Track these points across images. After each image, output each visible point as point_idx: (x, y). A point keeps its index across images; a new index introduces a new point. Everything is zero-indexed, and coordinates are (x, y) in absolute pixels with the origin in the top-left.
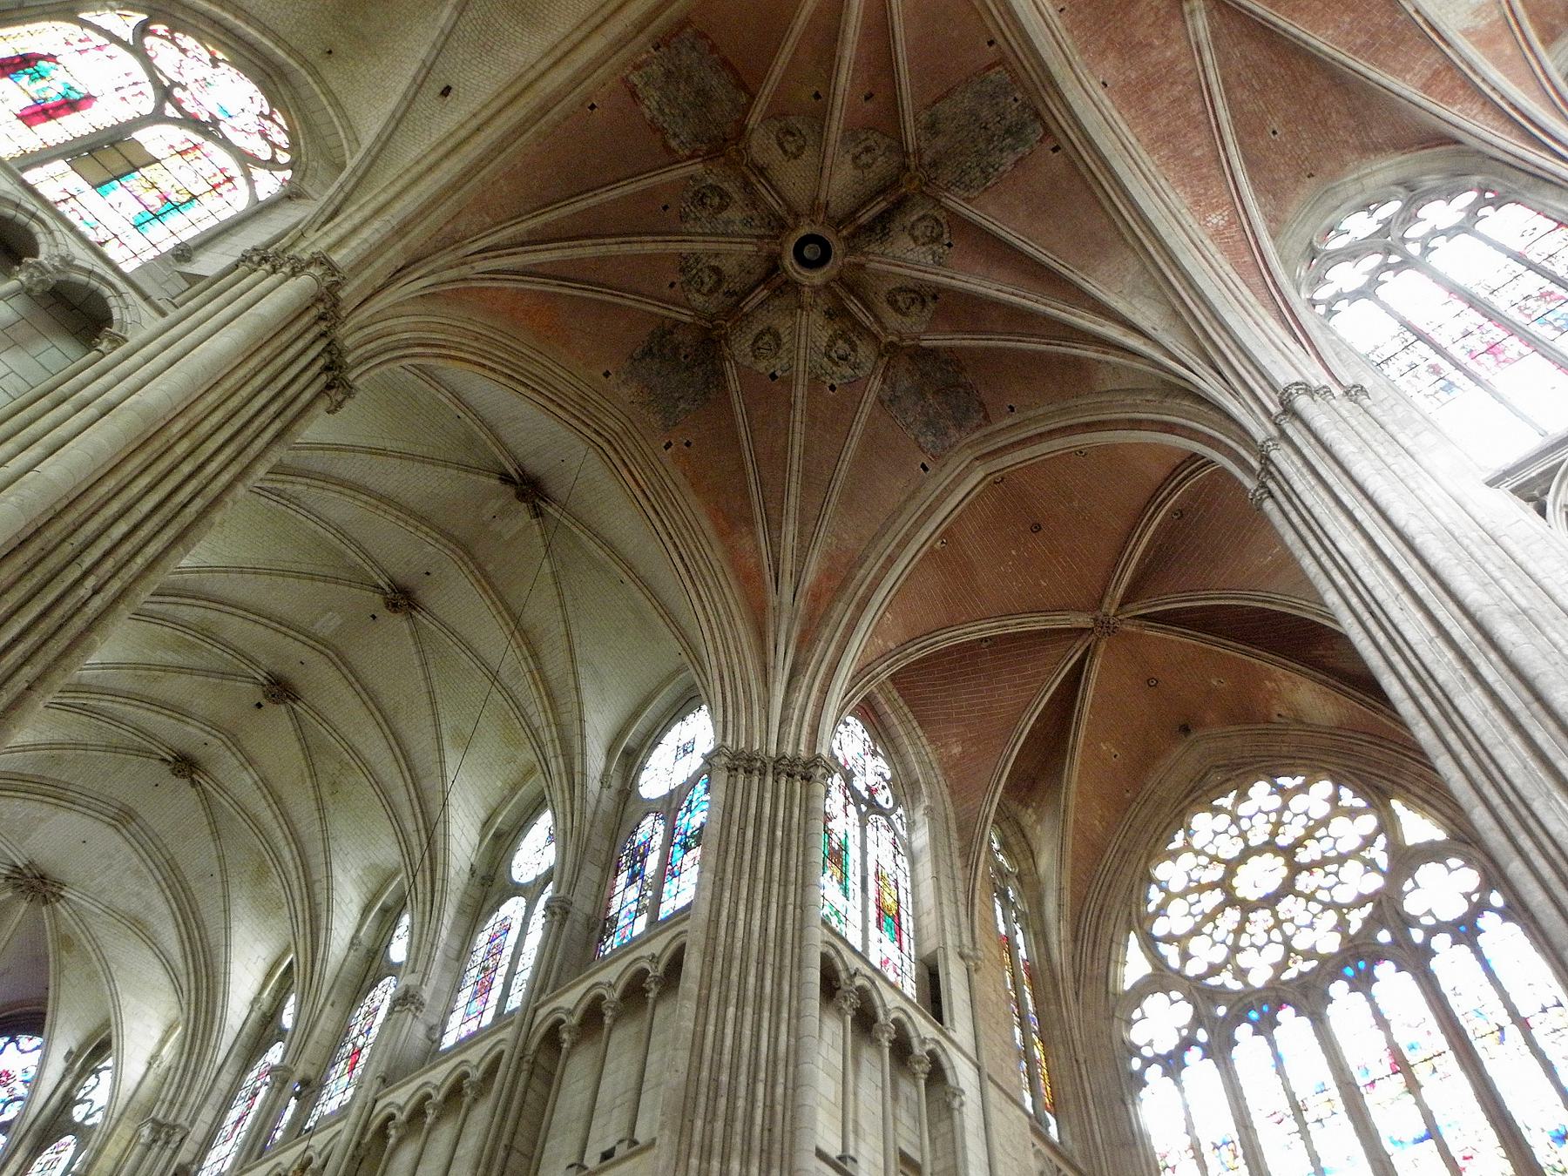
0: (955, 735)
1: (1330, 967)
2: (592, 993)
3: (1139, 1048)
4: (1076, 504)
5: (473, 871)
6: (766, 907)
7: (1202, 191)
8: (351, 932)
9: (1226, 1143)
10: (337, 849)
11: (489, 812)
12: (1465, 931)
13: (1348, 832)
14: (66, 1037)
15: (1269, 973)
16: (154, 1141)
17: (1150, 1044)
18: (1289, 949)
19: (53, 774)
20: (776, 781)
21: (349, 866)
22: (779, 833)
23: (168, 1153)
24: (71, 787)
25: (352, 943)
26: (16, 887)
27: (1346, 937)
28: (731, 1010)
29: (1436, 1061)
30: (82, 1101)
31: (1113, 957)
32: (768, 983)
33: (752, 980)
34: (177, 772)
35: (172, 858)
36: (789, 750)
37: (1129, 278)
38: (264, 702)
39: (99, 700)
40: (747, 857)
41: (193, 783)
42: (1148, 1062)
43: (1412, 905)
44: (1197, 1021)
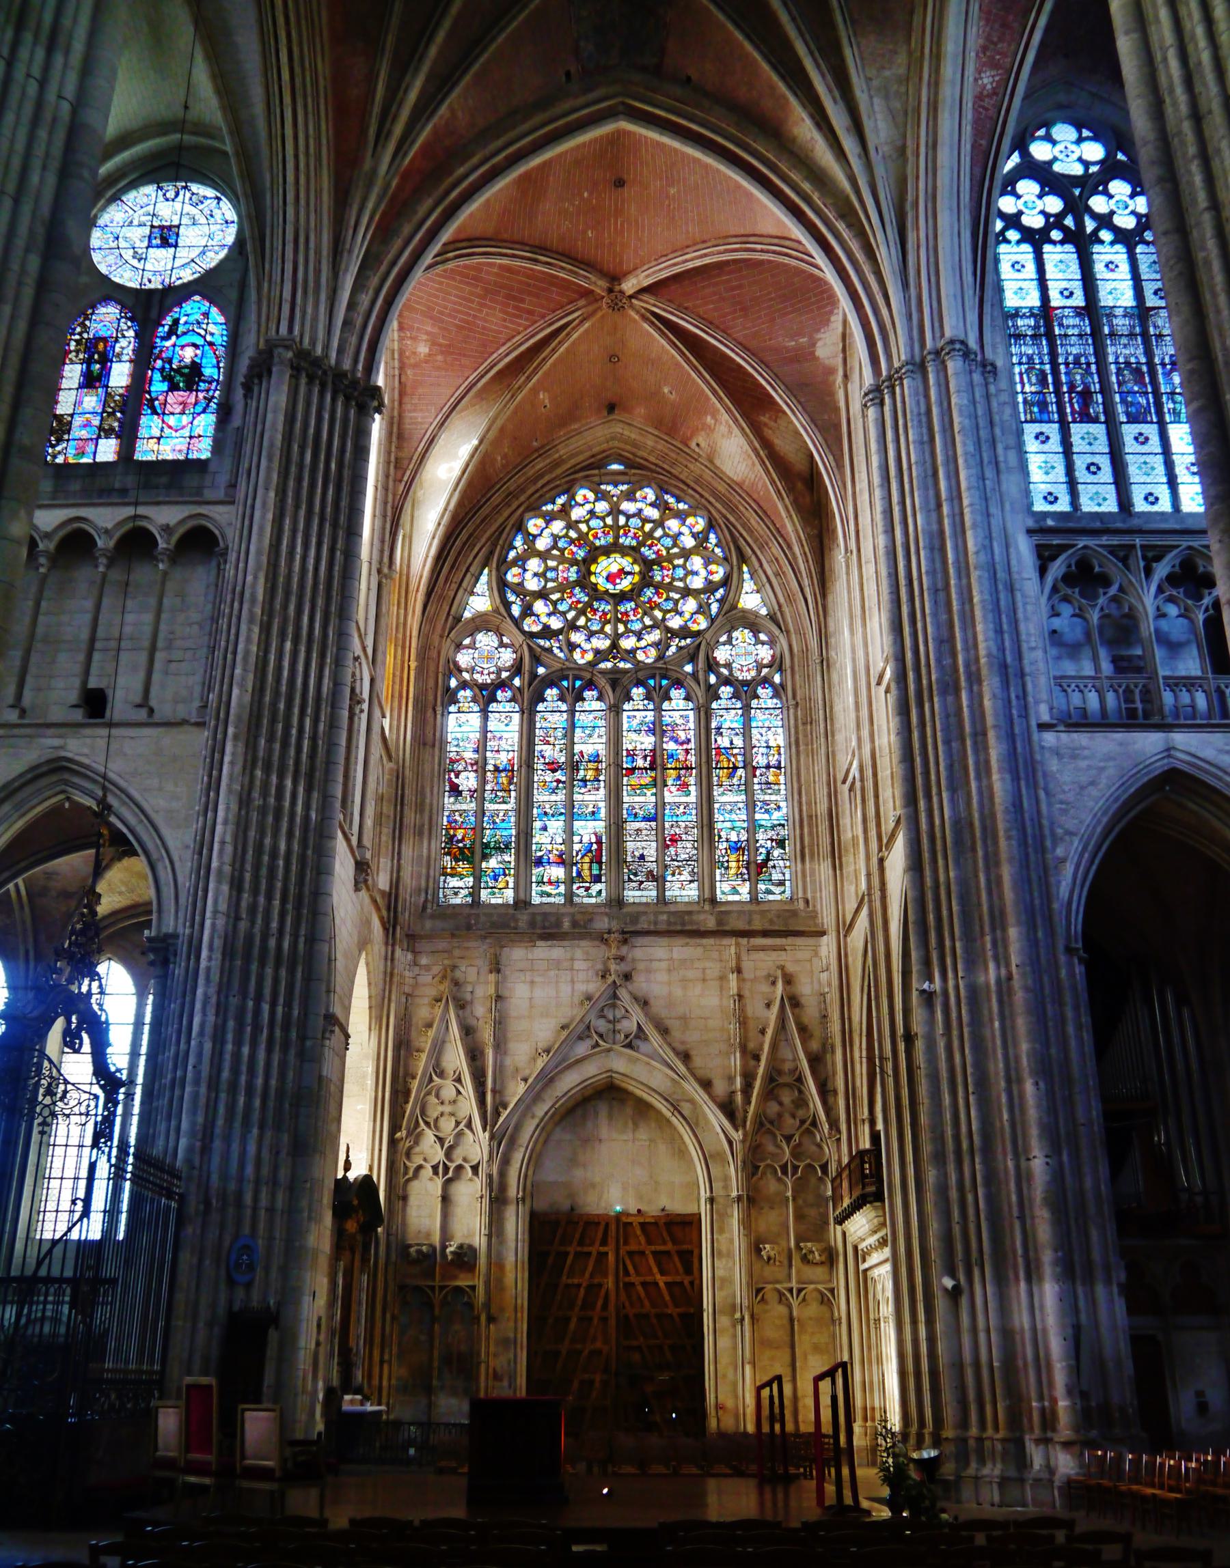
0: (427, 333)
1: (641, 675)
2: (76, 525)
3: (460, 670)
4: (672, 191)
7: (995, 39)
9: (505, 770)
12: (745, 691)
13: (699, 573)
15: (589, 657)
17: (471, 670)
18: (615, 645)
20: (334, 400)
22: (333, 466)
27: (660, 657)
28: (288, 645)
29: (683, 772)
31: (464, 584)
32: (317, 625)
36: (347, 365)
37: (887, 73)
40: (305, 484)
42: (464, 685)
43: (721, 654)
44: (517, 669)
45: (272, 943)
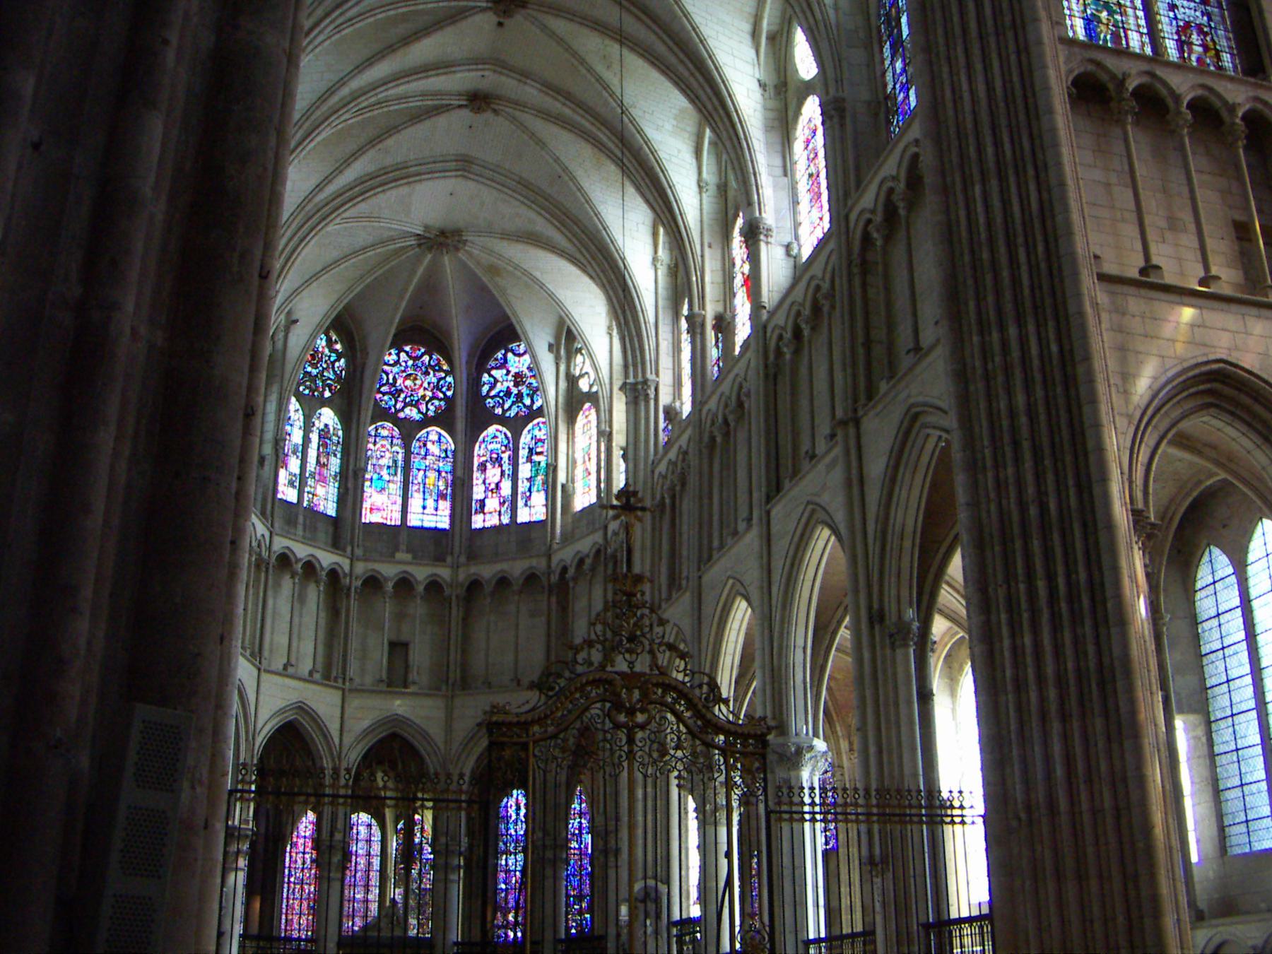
5: (762, 85)
6: (987, 67)
8: (694, 178)
10: (640, 113)
11: (752, 20)
14: (540, 337)
16: (636, 398)
19: (388, 161)
21: (660, 123)
23: (652, 403)
24: (410, 164)
25: (700, 187)
26: (430, 249)
30: (581, 376)
33: (990, 150)
34: (478, 110)
35: (521, 177)
38: (502, 20)
39: (376, 94)
41: (495, 111)
45: (1033, 511)
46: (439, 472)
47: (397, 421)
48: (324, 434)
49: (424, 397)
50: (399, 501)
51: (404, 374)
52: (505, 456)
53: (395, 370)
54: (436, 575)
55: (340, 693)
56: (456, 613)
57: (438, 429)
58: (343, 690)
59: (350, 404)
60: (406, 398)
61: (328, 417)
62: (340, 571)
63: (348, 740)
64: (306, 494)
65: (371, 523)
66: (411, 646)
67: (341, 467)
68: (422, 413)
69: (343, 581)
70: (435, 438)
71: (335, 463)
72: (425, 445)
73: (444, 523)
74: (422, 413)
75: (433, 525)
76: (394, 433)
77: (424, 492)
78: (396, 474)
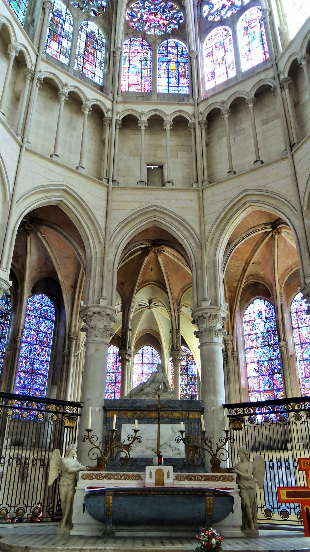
46: (178, 63)
47: (144, 36)
48: (90, 36)
49: (163, 24)
50: (150, 80)
51: (148, 13)
52: (227, 42)
53: (143, 11)
54: (180, 111)
55: (106, 189)
56: (200, 134)
57: (175, 40)
58: (108, 187)
59: (110, 24)
60: (151, 24)
61: (93, 27)
62: (103, 108)
63: (113, 225)
64: (76, 64)
65: (128, 92)
66: (165, 167)
67: (105, 59)
68: (163, 31)
69: (106, 115)
70: (174, 45)
71: (101, 56)
72: (167, 48)
73: (186, 91)
74: (163, 31)
75: (177, 92)
76: (144, 43)
77: (168, 74)
78: (146, 65)
